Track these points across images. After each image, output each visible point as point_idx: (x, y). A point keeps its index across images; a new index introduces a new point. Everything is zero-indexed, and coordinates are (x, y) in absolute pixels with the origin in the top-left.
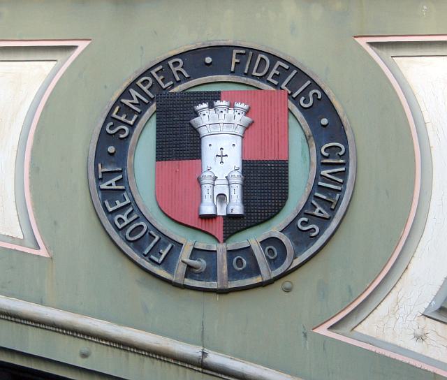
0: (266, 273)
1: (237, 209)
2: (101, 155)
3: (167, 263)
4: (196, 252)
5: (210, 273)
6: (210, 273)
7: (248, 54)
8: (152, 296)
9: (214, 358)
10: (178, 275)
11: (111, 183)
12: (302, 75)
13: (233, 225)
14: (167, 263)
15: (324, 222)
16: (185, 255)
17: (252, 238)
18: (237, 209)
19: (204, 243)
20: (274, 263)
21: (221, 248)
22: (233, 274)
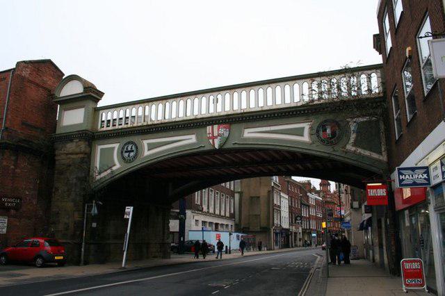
13: (331, 138)
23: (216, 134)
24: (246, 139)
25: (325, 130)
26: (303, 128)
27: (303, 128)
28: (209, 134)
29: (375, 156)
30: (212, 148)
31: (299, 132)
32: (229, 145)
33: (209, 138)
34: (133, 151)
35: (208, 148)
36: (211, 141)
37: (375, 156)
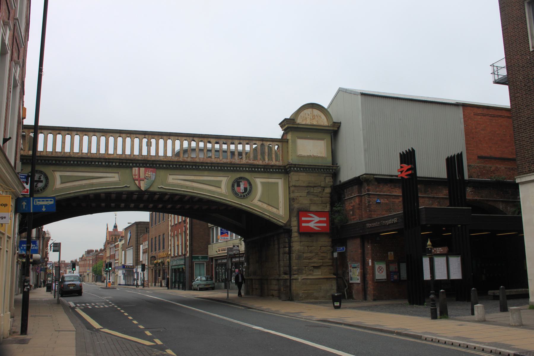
0: (246, 197)
1: (243, 191)
2: (232, 186)
3: (238, 196)
4: (240, 195)
5: (241, 197)
6: (241, 197)
7: (244, 178)
8: (237, 199)
9: (242, 204)
10: (239, 197)
11: (233, 189)
12: (248, 180)
13: (243, 193)
14: (238, 196)
15: (250, 193)
16: (239, 195)
17: (245, 194)
18: (243, 191)
19: (241, 194)
20: (246, 196)
21: (242, 195)
22: (243, 197)
23: (142, 176)
24: (169, 185)
25: (239, 186)
26: (221, 181)
27: (221, 181)
28: (135, 175)
29: (274, 210)
30: (137, 189)
31: (217, 185)
32: (154, 189)
33: (134, 180)
34: (42, 182)
35: (133, 188)
36: (137, 182)
37: (274, 210)
